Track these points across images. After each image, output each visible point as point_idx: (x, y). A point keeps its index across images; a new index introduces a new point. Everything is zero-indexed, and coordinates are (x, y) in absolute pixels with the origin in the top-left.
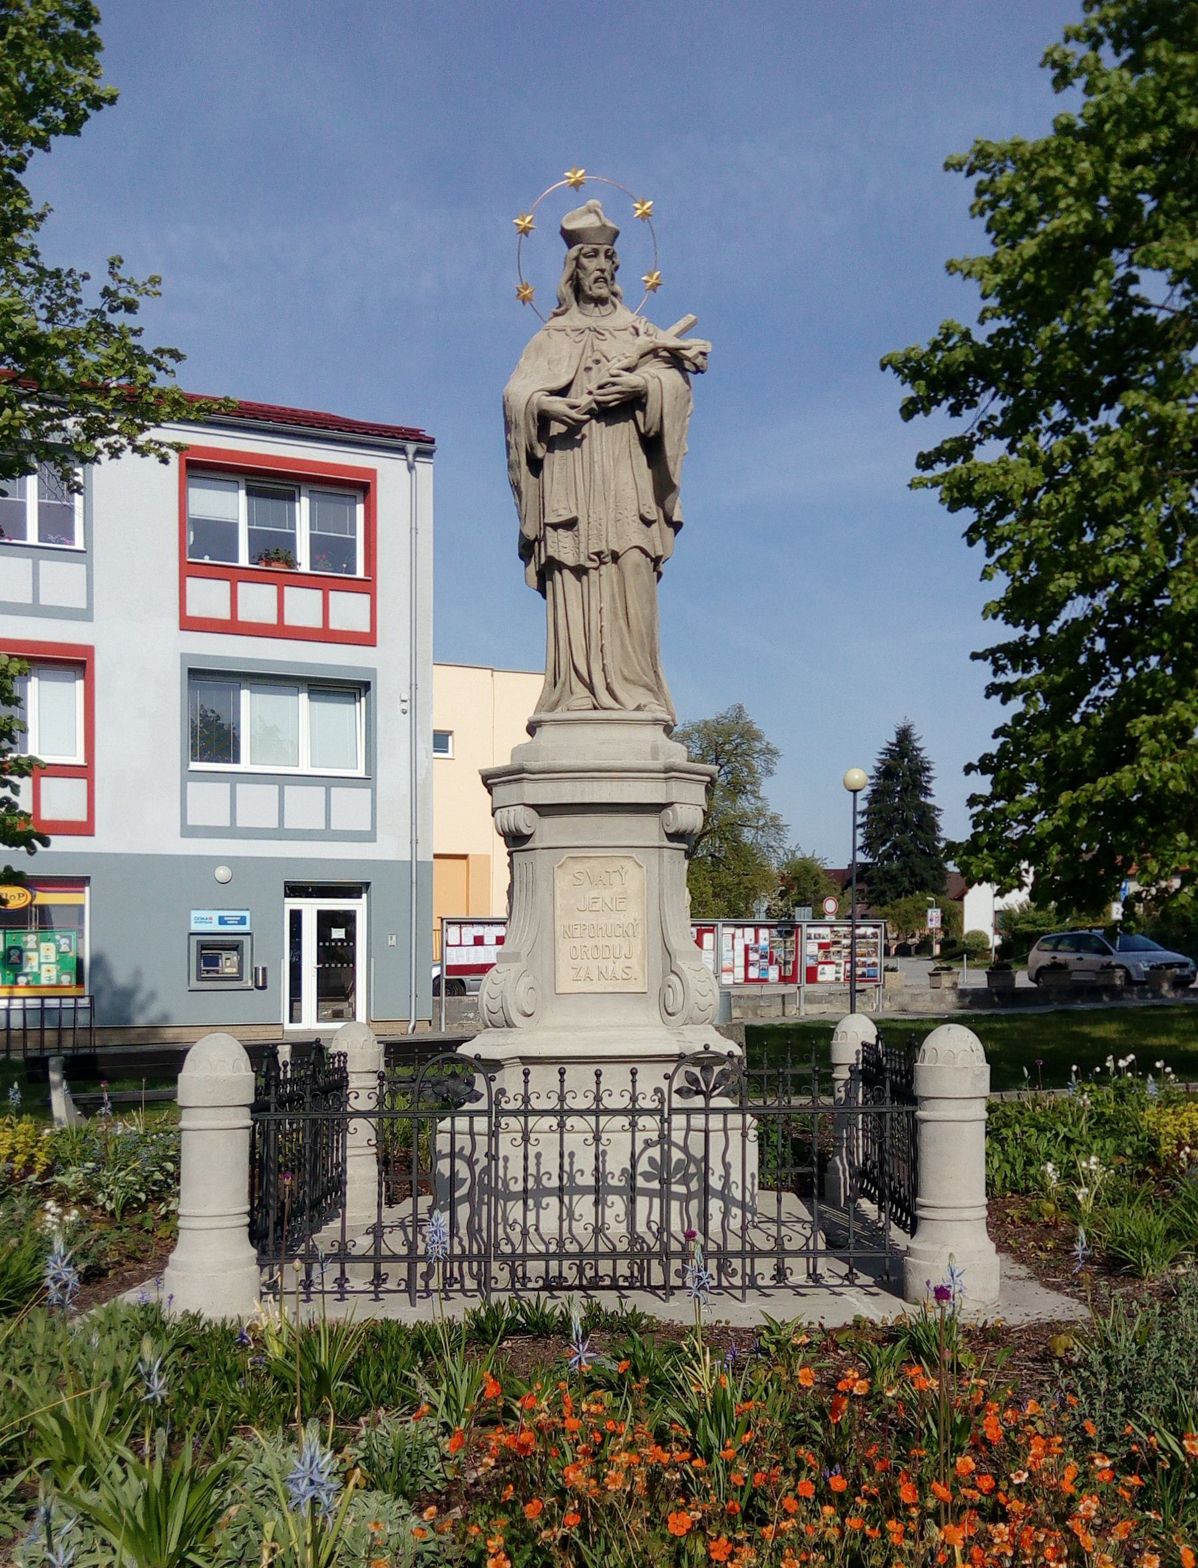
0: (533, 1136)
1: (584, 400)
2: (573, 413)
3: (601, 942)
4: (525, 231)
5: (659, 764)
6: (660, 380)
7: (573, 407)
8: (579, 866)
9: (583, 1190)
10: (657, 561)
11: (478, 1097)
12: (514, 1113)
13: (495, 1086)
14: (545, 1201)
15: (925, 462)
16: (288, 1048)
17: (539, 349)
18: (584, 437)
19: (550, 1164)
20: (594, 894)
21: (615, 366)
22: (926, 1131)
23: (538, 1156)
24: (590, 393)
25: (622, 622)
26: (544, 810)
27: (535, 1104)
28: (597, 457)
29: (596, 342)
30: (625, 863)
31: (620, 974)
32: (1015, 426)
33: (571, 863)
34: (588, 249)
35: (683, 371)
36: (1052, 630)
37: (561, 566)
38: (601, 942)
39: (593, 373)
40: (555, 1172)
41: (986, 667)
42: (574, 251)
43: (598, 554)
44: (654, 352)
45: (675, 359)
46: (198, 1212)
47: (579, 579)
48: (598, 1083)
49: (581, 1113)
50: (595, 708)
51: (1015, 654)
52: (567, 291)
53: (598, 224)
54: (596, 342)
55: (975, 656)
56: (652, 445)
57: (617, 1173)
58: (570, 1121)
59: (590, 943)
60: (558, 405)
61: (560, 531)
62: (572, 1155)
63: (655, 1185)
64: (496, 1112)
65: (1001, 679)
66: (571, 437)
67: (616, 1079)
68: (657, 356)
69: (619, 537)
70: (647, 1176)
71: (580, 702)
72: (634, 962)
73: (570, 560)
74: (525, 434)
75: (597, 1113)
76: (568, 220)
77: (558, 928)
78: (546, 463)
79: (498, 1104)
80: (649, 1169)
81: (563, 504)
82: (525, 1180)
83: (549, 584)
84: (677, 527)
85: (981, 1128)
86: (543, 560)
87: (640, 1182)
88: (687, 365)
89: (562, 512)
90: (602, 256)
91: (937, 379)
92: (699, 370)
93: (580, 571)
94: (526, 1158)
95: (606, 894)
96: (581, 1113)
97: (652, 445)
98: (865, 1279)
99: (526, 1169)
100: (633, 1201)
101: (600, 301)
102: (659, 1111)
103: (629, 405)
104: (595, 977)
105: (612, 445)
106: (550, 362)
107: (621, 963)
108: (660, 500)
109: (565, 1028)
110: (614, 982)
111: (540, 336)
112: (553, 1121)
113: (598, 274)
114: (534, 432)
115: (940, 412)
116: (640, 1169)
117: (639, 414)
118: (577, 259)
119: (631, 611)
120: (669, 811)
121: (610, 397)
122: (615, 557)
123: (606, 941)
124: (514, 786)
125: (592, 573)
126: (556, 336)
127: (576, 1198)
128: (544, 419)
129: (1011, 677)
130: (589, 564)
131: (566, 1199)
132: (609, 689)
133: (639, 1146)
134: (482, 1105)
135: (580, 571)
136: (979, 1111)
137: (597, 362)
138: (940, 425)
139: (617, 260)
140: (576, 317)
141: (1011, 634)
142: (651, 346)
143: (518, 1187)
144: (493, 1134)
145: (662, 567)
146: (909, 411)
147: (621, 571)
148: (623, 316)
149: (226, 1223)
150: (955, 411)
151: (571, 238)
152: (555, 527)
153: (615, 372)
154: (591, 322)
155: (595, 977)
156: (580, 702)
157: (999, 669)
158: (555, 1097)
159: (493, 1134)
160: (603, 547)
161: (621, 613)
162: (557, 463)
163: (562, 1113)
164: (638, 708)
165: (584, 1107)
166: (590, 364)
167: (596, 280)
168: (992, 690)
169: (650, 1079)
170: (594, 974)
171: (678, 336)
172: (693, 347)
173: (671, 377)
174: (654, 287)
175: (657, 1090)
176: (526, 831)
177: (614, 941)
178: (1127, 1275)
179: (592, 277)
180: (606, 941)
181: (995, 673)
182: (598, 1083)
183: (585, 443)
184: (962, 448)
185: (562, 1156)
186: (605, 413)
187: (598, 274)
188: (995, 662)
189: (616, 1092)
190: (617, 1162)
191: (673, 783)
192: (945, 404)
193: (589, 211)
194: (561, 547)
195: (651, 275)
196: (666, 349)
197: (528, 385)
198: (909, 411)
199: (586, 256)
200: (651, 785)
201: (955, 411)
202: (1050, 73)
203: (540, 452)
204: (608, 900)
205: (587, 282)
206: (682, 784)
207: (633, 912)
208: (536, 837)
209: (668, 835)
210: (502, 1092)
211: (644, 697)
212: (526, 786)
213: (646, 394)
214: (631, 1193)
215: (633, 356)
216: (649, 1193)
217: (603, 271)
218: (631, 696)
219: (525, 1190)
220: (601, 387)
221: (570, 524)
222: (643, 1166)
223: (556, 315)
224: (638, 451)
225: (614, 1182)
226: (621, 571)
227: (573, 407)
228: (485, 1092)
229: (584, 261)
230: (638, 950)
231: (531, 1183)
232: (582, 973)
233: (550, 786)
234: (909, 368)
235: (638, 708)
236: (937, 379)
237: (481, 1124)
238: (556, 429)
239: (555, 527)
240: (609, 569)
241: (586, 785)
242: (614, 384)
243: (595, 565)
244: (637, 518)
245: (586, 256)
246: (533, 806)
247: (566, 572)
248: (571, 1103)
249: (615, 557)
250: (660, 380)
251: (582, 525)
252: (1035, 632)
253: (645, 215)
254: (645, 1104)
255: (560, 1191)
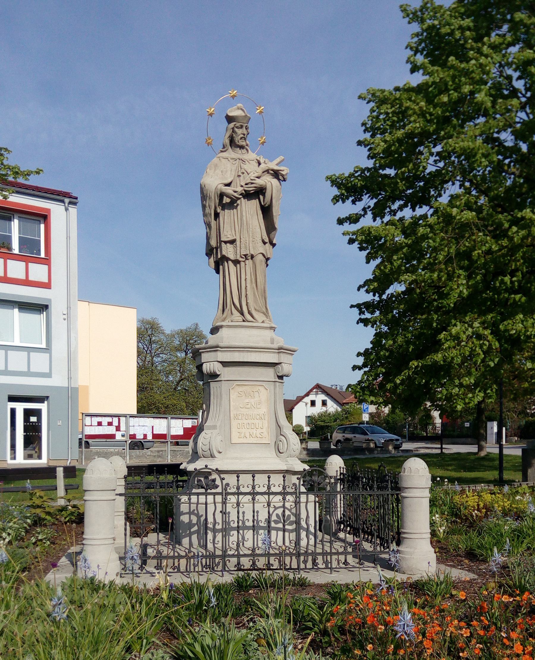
0: (241, 505)
1: (240, 189)
2: (235, 194)
3: (250, 421)
4: (211, 115)
5: (276, 346)
6: (268, 181)
7: (235, 192)
8: (240, 389)
9: (248, 528)
10: (267, 259)
11: (217, 487)
12: (233, 494)
13: (224, 482)
14: (232, 533)
15: (340, 222)
16: (62, 469)
17: (216, 166)
18: (238, 205)
19: (249, 516)
20: (247, 401)
21: (252, 176)
22: (406, 501)
23: (244, 513)
24: (242, 186)
25: (254, 285)
26: (225, 364)
27: (242, 490)
28: (244, 214)
29: (242, 165)
30: (260, 388)
31: (259, 436)
32: (378, 212)
33: (237, 387)
34: (238, 125)
35: (279, 180)
36: (384, 297)
37: (228, 259)
38: (250, 421)
39: (242, 178)
40: (251, 519)
41: (356, 311)
42: (232, 125)
43: (245, 255)
44: (267, 171)
45: (276, 174)
46: (95, 537)
47: (236, 266)
48: (269, 481)
49: (262, 494)
50: (244, 321)
51: (368, 306)
52: (227, 142)
53: (243, 114)
54: (242, 165)
55: (352, 306)
56: (267, 211)
57: (263, 521)
58: (258, 497)
59: (246, 422)
60: (229, 190)
61: (228, 244)
62: (258, 512)
63: (280, 525)
64: (225, 494)
65: (363, 317)
66: (232, 204)
67: (261, 480)
68: (268, 173)
69: (254, 248)
70: (276, 522)
71: (237, 318)
72: (264, 430)
73: (232, 257)
74: (213, 202)
75: (269, 494)
76: (230, 112)
77: (232, 415)
78: (220, 215)
79: (226, 490)
80: (276, 519)
81: (230, 233)
82: (238, 522)
83: (221, 267)
84: (274, 245)
85: (428, 500)
86: (219, 256)
87: (273, 525)
88: (281, 177)
89: (229, 236)
90: (244, 128)
91: (348, 188)
92: (284, 180)
93: (236, 262)
94: (238, 513)
95: (252, 401)
96: (262, 494)
97: (267, 211)
98: (367, 564)
99: (238, 518)
100: (269, 532)
101: (242, 147)
102: (295, 493)
103: (258, 193)
104: (248, 437)
105: (250, 209)
106: (221, 173)
107: (259, 431)
108: (268, 234)
109: (236, 458)
110: (256, 439)
111: (215, 160)
112: (250, 497)
113: (242, 136)
114: (217, 201)
115: (349, 202)
116: (272, 519)
117: (261, 197)
118: (233, 128)
119: (258, 280)
120: (279, 366)
121: (251, 188)
122: (252, 257)
123: (253, 421)
124: (213, 353)
125: (242, 264)
126: (223, 160)
127: (246, 531)
128: (222, 195)
129: (368, 315)
130: (241, 259)
131: (241, 532)
132: (249, 313)
133: (271, 510)
134: (219, 490)
135: (236, 262)
136: (427, 494)
137: (243, 173)
138: (348, 208)
139: (249, 130)
140: (231, 153)
141: (369, 297)
142: (267, 168)
143: (236, 525)
144: (224, 503)
145: (269, 262)
146: (336, 200)
147: (254, 264)
148: (252, 155)
149: (107, 542)
150: (354, 202)
151: (230, 119)
152: (226, 242)
153: (253, 178)
154: (241, 157)
155: (248, 437)
156: (237, 318)
157: (361, 313)
158: (250, 487)
159: (224, 503)
160: (248, 253)
161: (254, 281)
162: (226, 215)
163: (254, 494)
164: (263, 322)
165: (263, 491)
166: (240, 174)
167: (241, 138)
168: (361, 321)
169: (277, 481)
170: (248, 435)
171: (277, 165)
172: (285, 170)
173: (275, 182)
174: (263, 143)
175: (294, 484)
176: (218, 373)
177: (256, 421)
178: (482, 561)
179: (239, 137)
180: (253, 421)
181: (360, 314)
182: (269, 481)
183: (239, 207)
184: (354, 219)
185: (254, 512)
186: (248, 195)
187: (242, 136)
188: (360, 309)
189: (277, 485)
190: (263, 516)
191: (281, 354)
192: (351, 199)
193: (238, 108)
194: (228, 251)
195: (262, 138)
196: (272, 170)
197: (214, 181)
198: (336, 200)
199: (237, 127)
200: (272, 355)
201: (354, 202)
202: (409, 66)
203: (219, 210)
204: (253, 404)
205: (237, 139)
206: (285, 355)
207: (263, 409)
208: (222, 375)
209: (278, 376)
210: (228, 485)
211: (264, 318)
212: (219, 353)
213: (265, 189)
214: (269, 529)
215: (260, 173)
216: (278, 529)
217: (244, 135)
218: (259, 317)
219: (238, 527)
220: (246, 184)
221: (232, 242)
222: (274, 518)
223: (222, 151)
224: (260, 212)
225: (262, 524)
226: (254, 264)
227: (235, 192)
228: (220, 484)
229: (236, 130)
230: (266, 425)
231: (240, 524)
232: (243, 435)
233: (257, 354)
234: (335, 182)
235: (263, 322)
236: (348, 188)
237: (219, 498)
238: (226, 200)
239: (226, 242)
240: (249, 262)
241: (253, 354)
242: (252, 183)
243: (243, 260)
244: (261, 241)
245: (237, 128)
246: (221, 362)
247: (230, 262)
248: (257, 490)
249: (252, 257)
250: (268, 181)
251: (238, 243)
252: (377, 298)
253: (261, 112)
254: (289, 490)
255: (238, 528)
